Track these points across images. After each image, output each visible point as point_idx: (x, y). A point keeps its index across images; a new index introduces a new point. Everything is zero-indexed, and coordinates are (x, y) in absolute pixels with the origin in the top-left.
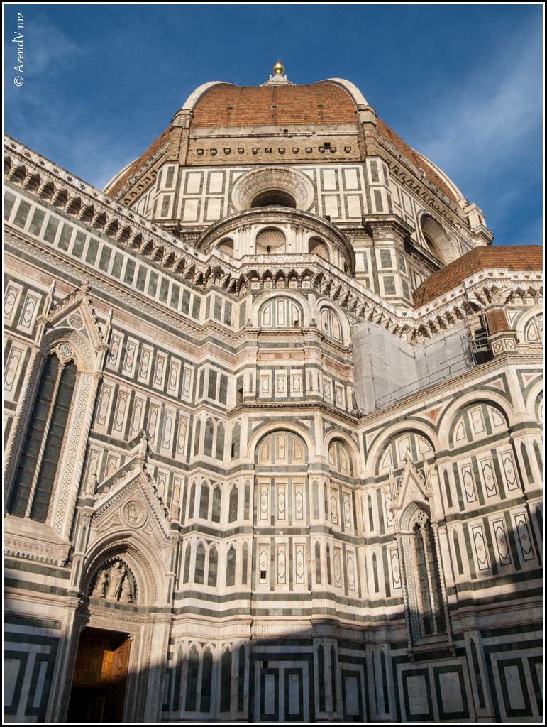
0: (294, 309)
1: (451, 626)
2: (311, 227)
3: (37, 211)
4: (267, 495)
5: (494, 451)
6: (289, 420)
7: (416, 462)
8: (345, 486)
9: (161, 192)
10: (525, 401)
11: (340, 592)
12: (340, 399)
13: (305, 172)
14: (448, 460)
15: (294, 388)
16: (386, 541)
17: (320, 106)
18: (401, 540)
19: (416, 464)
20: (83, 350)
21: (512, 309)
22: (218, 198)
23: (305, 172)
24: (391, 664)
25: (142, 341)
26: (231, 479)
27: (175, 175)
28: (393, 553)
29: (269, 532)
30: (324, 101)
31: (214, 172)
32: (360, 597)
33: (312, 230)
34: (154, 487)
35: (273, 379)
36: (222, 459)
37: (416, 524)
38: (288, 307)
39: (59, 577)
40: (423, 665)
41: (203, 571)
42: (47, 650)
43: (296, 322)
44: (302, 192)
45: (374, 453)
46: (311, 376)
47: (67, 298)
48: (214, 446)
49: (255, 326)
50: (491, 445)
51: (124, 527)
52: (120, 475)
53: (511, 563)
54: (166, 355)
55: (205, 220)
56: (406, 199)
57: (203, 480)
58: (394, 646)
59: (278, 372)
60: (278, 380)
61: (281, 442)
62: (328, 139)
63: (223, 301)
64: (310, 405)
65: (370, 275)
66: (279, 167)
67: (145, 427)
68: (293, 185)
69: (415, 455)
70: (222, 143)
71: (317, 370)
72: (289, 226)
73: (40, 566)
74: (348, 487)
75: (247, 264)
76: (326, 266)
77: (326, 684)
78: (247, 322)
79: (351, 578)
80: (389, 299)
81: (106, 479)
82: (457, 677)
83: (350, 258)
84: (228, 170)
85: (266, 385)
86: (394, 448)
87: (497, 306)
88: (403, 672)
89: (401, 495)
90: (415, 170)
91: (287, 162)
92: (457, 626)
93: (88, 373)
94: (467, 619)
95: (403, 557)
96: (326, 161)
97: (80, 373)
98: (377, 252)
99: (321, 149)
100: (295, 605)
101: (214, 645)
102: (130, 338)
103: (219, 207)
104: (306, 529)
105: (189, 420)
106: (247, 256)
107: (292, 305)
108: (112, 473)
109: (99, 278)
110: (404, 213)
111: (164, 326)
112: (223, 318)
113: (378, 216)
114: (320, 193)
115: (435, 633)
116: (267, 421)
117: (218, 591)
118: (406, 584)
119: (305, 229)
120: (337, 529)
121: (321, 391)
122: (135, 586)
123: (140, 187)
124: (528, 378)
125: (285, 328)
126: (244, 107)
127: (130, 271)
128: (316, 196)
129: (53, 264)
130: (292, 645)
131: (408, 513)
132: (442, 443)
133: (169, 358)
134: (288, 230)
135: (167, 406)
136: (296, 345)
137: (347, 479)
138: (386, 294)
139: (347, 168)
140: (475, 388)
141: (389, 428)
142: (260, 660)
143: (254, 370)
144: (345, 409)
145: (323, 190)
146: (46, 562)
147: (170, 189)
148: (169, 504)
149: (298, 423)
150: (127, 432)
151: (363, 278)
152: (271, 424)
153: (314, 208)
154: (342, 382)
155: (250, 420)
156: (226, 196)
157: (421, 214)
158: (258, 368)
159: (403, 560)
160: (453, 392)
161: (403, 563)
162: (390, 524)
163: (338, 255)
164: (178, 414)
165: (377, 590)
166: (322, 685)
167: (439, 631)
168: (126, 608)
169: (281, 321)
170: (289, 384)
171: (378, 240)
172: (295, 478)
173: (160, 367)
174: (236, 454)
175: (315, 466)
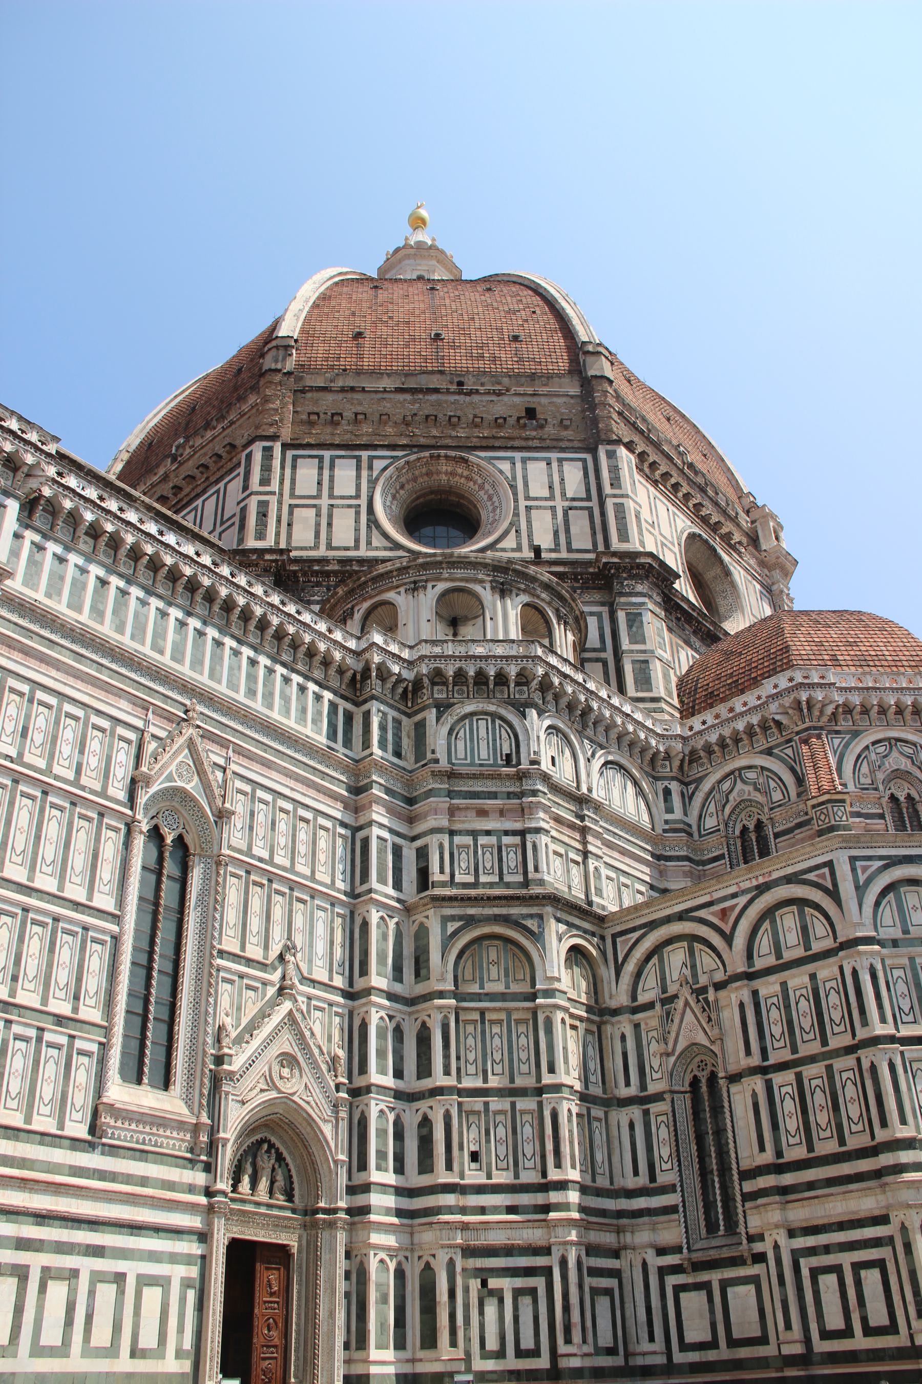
1: (746, 1223)
2: (523, 586)
4: (475, 1038)
5: (813, 977)
7: (697, 986)
16: (650, 1102)
19: (696, 989)
20: (195, 817)
21: (837, 732)
22: (350, 506)
24: (657, 1276)
26: (418, 1011)
28: (660, 1119)
32: (612, 1183)
33: (524, 591)
35: (476, 852)
37: (695, 1077)
38: (494, 729)
40: (704, 1277)
43: (508, 756)
44: (490, 498)
45: (630, 968)
49: (444, 764)
50: (810, 968)
51: (274, 1094)
53: (832, 1137)
55: (329, 547)
56: (662, 509)
58: (661, 1251)
59: (482, 840)
61: (493, 955)
62: (533, 402)
64: (537, 897)
65: (609, 655)
67: (289, 939)
68: (475, 483)
69: (695, 975)
72: (488, 586)
75: (426, 656)
76: (553, 660)
77: (572, 1308)
78: (429, 756)
79: (599, 1157)
82: (754, 1290)
83: (580, 631)
84: (365, 454)
86: (661, 961)
88: (674, 1287)
89: (673, 1035)
92: (755, 1222)
94: (770, 1214)
95: (675, 1125)
96: (530, 443)
98: (621, 616)
99: (522, 421)
100: (525, 1199)
101: (406, 1258)
104: (536, 1088)
105: (348, 919)
106: (426, 641)
107: (500, 726)
110: (659, 538)
112: (390, 747)
114: (522, 503)
115: (721, 1233)
116: (470, 921)
117: (407, 1180)
121: (552, 872)
122: (291, 1177)
123: (201, 469)
124: (864, 869)
130: (521, 1255)
131: (684, 1061)
134: (486, 594)
136: (509, 795)
138: (637, 691)
140: (789, 879)
141: (655, 931)
142: (476, 1277)
145: (527, 498)
147: (267, 489)
149: (516, 924)
150: (266, 947)
151: (597, 660)
152: (476, 928)
153: (513, 531)
155: (445, 920)
156: (363, 502)
158: (452, 833)
159: (676, 1130)
160: (755, 883)
161: (676, 1135)
162: (655, 1076)
165: (636, 1173)
166: (566, 1308)
167: (726, 1230)
170: (500, 860)
171: (622, 594)
172: (515, 1012)
174: (423, 972)
175: (549, 993)
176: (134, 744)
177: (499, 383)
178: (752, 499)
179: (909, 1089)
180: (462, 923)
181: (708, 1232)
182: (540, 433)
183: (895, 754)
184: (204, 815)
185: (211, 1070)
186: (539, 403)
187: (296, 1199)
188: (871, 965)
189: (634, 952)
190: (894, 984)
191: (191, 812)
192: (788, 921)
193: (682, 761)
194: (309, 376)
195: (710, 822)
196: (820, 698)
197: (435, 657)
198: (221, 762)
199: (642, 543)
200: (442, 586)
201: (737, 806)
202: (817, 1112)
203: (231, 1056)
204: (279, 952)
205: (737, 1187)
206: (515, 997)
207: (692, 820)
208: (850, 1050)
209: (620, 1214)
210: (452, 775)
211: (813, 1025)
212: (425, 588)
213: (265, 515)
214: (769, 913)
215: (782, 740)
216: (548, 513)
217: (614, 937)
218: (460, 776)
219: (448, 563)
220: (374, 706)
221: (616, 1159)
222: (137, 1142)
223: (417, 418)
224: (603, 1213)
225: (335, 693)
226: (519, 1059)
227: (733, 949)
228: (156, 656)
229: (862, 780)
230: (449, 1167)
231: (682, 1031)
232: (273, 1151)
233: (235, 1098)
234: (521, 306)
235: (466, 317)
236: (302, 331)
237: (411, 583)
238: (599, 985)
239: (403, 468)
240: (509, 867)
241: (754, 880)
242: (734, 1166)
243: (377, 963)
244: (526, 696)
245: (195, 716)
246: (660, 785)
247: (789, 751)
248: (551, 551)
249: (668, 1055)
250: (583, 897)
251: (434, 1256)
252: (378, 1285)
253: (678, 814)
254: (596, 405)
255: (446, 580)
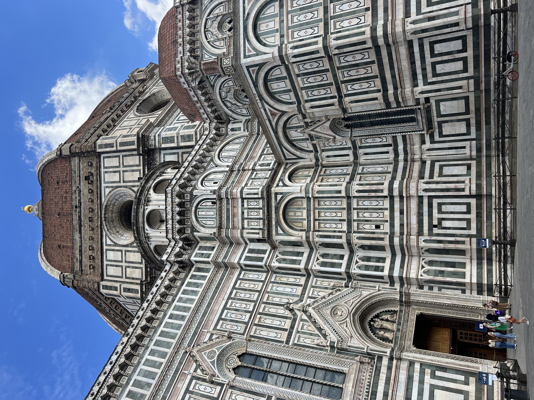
0: (204, 204)
1: (411, 106)
2: (146, 192)
3: (133, 385)
5: (298, 76)
6: (277, 208)
8: (320, 172)
9: (120, 294)
10: (265, 53)
11: (389, 176)
12: (264, 175)
13: (106, 194)
14: (304, 106)
15: (256, 205)
17: (58, 183)
18: (355, 137)
19: (306, 126)
21: (202, 55)
22: (125, 254)
23: (106, 194)
25: (225, 308)
26: (316, 247)
27: (109, 284)
29: (350, 223)
30: (53, 179)
31: (106, 257)
32: (392, 164)
33: (148, 191)
34: (322, 299)
36: (303, 253)
37: (345, 126)
39: (381, 364)
41: (376, 266)
42: (428, 371)
43: (213, 203)
44: (121, 196)
45: (298, 153)
46: (248, 194)
47: (196, 361)
48: (295, 258)
49: (215, 230)
51: (348, 319)
52: (314, 323)
54: (235, 291)
55: (141, 263)
56: (126, 124)
57: (316, 265)
58: (423, 142)
59: (246, 216)
60: (251, 215)
63: (199, 252)
64: (268, 195)
65: (180, 151)
66: (103, 212)
69: (300, 127)
70: (85, 252)
71: (244, 190)
72: (146, 207)
73: (374, 376)
74: (321, 170)
75: (173, 236)
76: (174, 182)
78: (212, 236)
79: (379, 169)
80: (196, 138)
81: (317, 332)
82: (443, 103)
84: (105, 247)
85: (254, 224)
86: (295, 140)
87: (200, 66)
89: (326, 136)
90: (105, 116)
91: (99, 206)
92: (411, 102)
93: (247, 346)
94: (406, 96)
95: (366, 136)
96: (99, 179)
97: (246, 351)
98: (163, 146)
100: (397, 206)
101: (423, 259)
102: (223, 317)
103: (131, 254)
104: (348, 199)
105: (277, 275)
106: (167, 236)
107: (201, 206)
108: (312, 328)
109: (182, 339)
110: (136, 126)
111: (215, 292)
112: (210, 252)
113: (138, 146)
114: (122, 184)
115: (415, 116)
116: (278, 223)
118: (384, 134)
119: (149, 196)
120: (348, 178)
121: (258, 187)
122: (386, 311)
123: (117, 308)
124: (249, 51)
125: (216, 210)
126: (58, 237)
127: (177, 317)
128: (124, 187)
129: (172, 372)
131: (338, 132)
132: (292, 109)
133: (236, 289)
134: (149, 208)
135: (269, 290)
136: (228, 203)
137: (316, 172)
138: (193, 141)
139: (104, 165)
140: (256, 86)
141: (283, 143)
142: (432, 230)
143: (245, 231)
144: (270, 172)
145: (120, 182)
146: (372, 372)
147: (119, 288)
148: (333, 289)
150: (286, 318)
151: (182, 156)
152: (280, 221)
153: (133, 188)
154: (252, 173)
155: (277, 234)
156: (124, 249)
157: (136, 113)
159: (368, 136)
160: (259, 101)
161: (370, 135)
162: (345, 143)
163: (166, 173)
164: (274, 283)
165: (388, 152)
167: (414, 114)
168: (400, 318)
169: (212, 213)
170: (254, 209)
173: (242, 295)
174: (299, 244)
175: (307, 192)
176: (197, 381)
177: (75, 191)
178: (127, 81)
179: (348, 30)
180: (278, 227)
181: (415, 121)
182: (95, 174)
183: (211, 29)
184: (230, 345)
185: (337, 352)
186: (83, 174)
187: (396, 309)
188: (291, 48)
189: (292, 152)
190: (301, 37)
191: (229, 351)
192: (275, 86)
193: (220, 123)
194: (75, 269)
195: (244, 111)
196: (187, 64)
197: (173, 233)
198: (209, 335)
199: (135, 135)
200: (147, 227)
201: (237, 100)
202: (359, 73)
203: (331, 342)
204: (289, 311)
205: (395, 110)
206: (309, 205)
207: (244, 119)
208: (330, 59)
209: (406, 160)
210: (220, 228)
211: (320, 76)
212: (147, 234)
213: (129, 289)
214: (272, 95)
215: (207, 80)
216: (126, 174)
217: (286, 159)
218: (221, 223)
219: (137, 224)
220: (193, 258)
221: (381, 161)
222: (368, 396)
223: (91, 225)
224: (405, 168)
225: (186, 276)
226: (335, 205)
227: (288, 111)
228: (163, 366)
229: (222, 45)
230: (382, 239)
231: (325, 132)
232: (374, 319)
233: (349, 341)
234: (47, 179)
235: (51, 202)
236: (59, 270)
237: (145, 239)
238: (306, 166)
239: (110, 232)
240: (256, 205)
241: (258, 102)
242: (385, 111)
243: (295, 264)
244: (188, 195)
245: (188, 348)
246: (230, 133)
247: (212, 78)
248: (140, 173)
249: (335, 138)
250: (270, 172)
251: (422, 248)
252: (436, 275)
253: (241, 125)
254: (81, 152)
255: (144, 225)
